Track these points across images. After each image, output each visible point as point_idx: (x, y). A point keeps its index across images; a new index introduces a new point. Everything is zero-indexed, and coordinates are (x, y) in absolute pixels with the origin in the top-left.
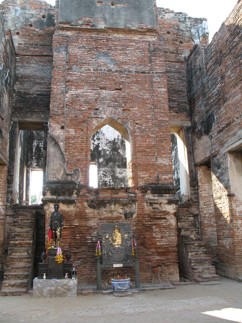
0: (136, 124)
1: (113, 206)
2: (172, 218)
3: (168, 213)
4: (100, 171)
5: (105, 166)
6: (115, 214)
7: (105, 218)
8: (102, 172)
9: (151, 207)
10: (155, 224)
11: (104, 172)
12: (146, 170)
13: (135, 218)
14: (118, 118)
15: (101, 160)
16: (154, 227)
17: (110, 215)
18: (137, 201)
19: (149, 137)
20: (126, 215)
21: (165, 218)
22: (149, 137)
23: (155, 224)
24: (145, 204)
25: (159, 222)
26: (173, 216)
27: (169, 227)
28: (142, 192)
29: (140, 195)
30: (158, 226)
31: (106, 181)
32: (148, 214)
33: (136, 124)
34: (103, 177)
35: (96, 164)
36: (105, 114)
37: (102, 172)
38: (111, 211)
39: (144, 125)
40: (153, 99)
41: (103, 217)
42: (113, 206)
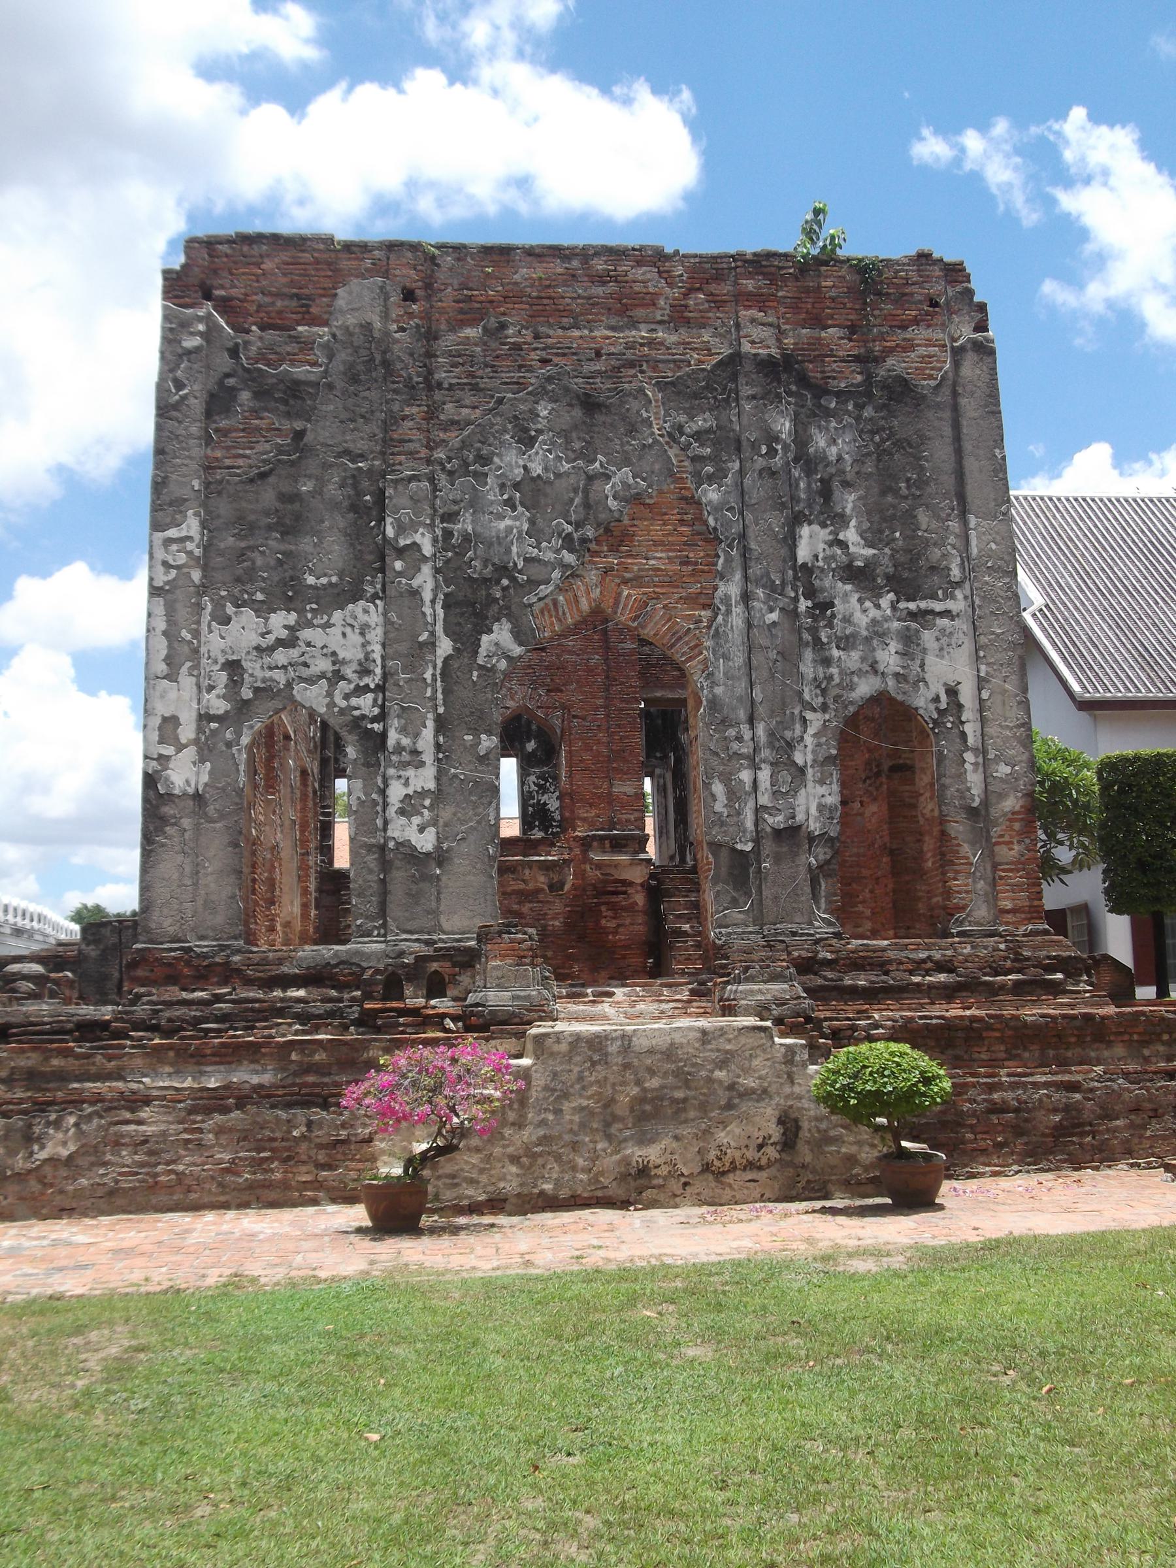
0: (575, 717)
1: (527, 872)
2: (637, 892)
3: (631, 884)
4: (529, 775)
5: (541, 763)
6: (531, 886)
7: (515, 892)
8: (533, 778)
9: (598, 873)
10: (604, 903)
11: (538, 778)
12: (591, 805)
13: (569, 892)
14: (539, 707)
15: (531, 746)
16: (603, 908)
17: (522, 886)
18: (572, 860)
19: (599, 742)
20: (552, 887)
21: (625, 893)
22: (599, 742)
23: (604, 903)
24: (588, 867)
25: (614, 899)
26: (639, 888)
27: (631, 908)
28: (583, 845)
29: (577, 851)
30: (614, 907)
31: (545, 804)
32: (593, 885)
33: (575, 717)
34: (537, 792)
35: (516, 756)
36: (512, 699)
37: (533, 778)
38: (523, 881)
39: (589, 718)
40: (607, 665)
41: (509, 889)
42: (527, 872)
